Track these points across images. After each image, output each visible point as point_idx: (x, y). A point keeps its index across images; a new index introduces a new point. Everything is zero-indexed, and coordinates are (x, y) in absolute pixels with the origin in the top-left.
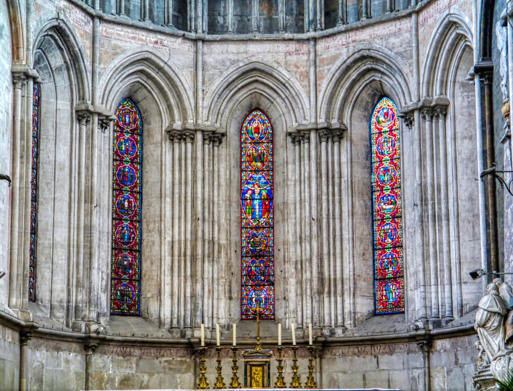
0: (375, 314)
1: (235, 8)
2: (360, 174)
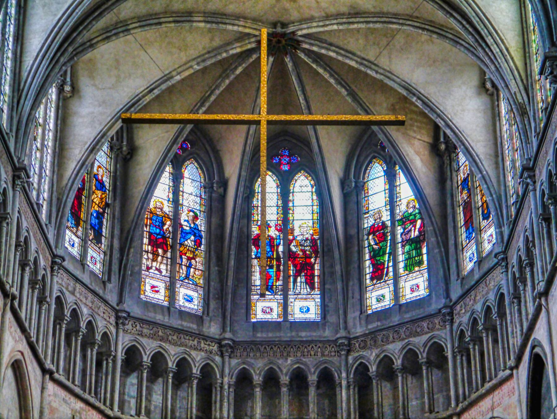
1: (263, 408)
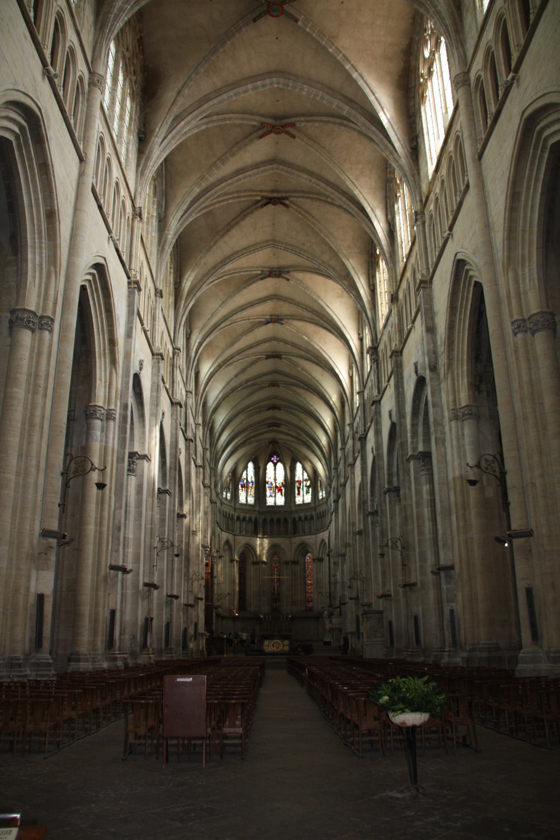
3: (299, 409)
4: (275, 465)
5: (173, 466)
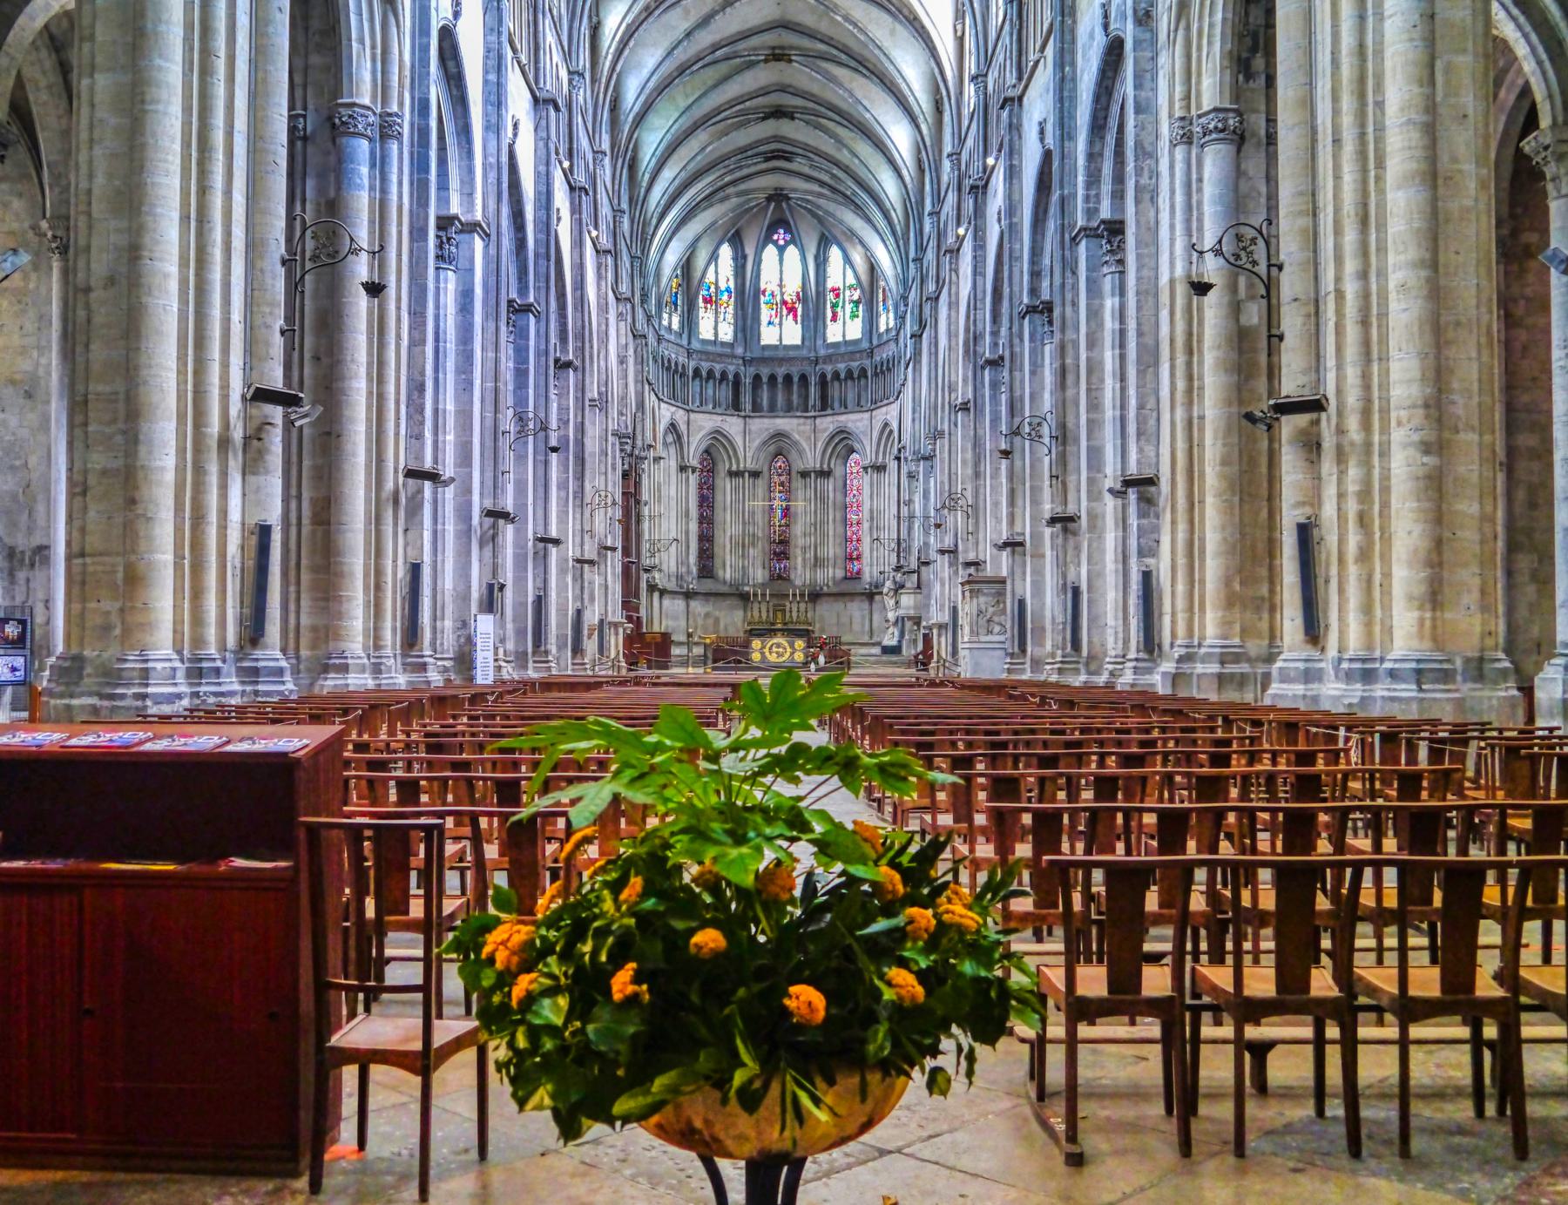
0: (846, 578)
2: (839, 497)
3: (837, 118)
4: (781, 250)
5: (542, 250)
